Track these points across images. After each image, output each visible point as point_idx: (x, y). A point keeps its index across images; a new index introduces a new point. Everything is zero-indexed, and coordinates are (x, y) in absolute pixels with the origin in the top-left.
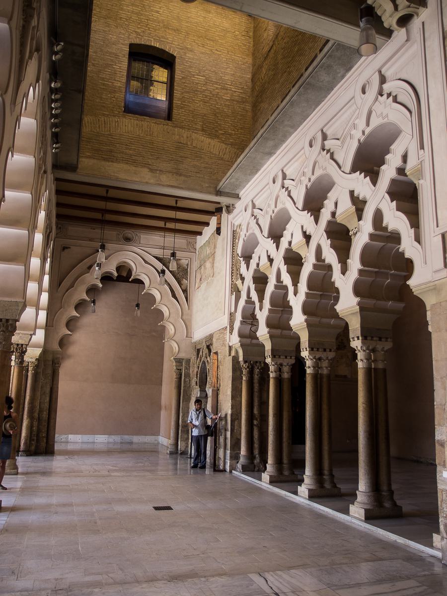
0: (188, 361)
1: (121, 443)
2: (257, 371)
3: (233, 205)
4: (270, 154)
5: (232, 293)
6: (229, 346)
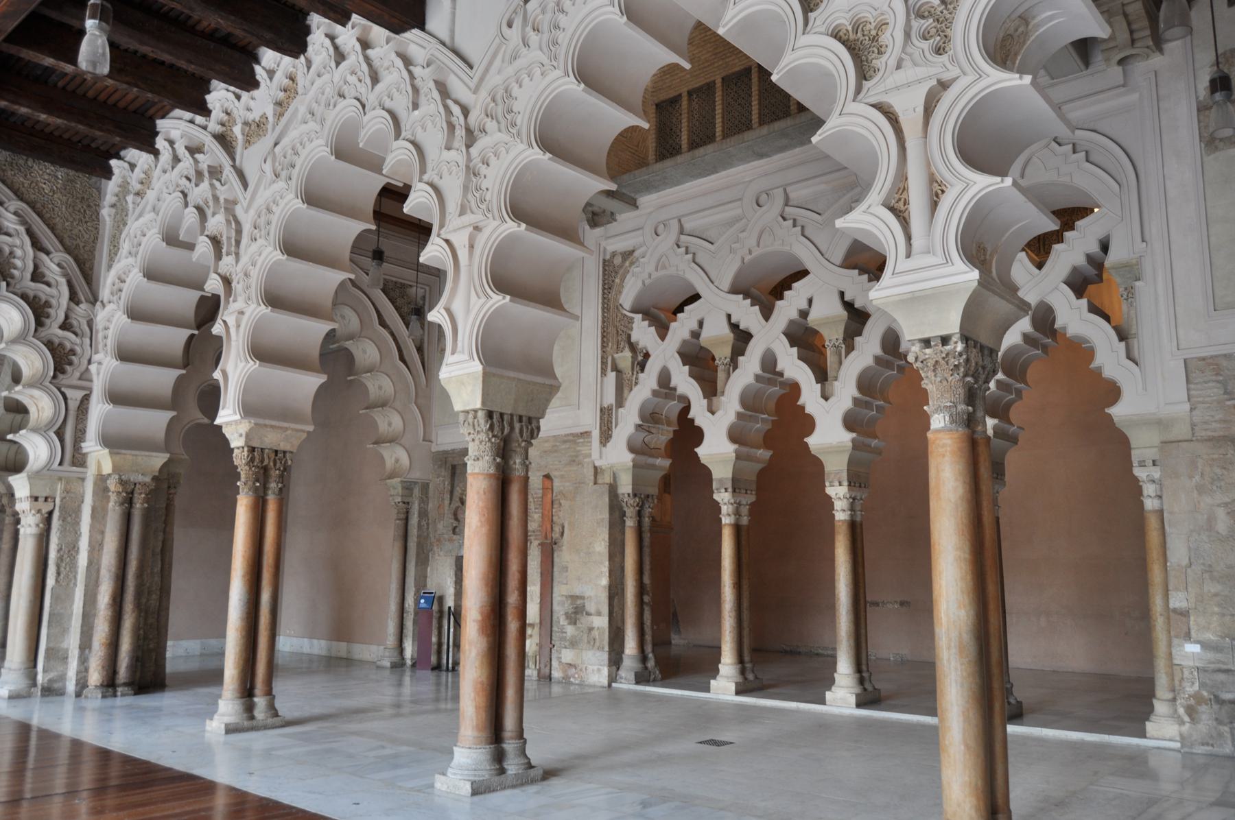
0: (425, 487)
1: (201, 655)
2: (647, 511)
3: (612, 214)
4: (761, 156)
5: (604, 372)
6: (596, 468)
